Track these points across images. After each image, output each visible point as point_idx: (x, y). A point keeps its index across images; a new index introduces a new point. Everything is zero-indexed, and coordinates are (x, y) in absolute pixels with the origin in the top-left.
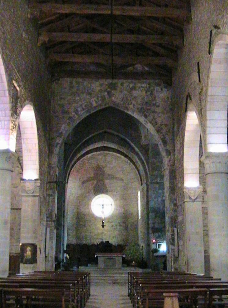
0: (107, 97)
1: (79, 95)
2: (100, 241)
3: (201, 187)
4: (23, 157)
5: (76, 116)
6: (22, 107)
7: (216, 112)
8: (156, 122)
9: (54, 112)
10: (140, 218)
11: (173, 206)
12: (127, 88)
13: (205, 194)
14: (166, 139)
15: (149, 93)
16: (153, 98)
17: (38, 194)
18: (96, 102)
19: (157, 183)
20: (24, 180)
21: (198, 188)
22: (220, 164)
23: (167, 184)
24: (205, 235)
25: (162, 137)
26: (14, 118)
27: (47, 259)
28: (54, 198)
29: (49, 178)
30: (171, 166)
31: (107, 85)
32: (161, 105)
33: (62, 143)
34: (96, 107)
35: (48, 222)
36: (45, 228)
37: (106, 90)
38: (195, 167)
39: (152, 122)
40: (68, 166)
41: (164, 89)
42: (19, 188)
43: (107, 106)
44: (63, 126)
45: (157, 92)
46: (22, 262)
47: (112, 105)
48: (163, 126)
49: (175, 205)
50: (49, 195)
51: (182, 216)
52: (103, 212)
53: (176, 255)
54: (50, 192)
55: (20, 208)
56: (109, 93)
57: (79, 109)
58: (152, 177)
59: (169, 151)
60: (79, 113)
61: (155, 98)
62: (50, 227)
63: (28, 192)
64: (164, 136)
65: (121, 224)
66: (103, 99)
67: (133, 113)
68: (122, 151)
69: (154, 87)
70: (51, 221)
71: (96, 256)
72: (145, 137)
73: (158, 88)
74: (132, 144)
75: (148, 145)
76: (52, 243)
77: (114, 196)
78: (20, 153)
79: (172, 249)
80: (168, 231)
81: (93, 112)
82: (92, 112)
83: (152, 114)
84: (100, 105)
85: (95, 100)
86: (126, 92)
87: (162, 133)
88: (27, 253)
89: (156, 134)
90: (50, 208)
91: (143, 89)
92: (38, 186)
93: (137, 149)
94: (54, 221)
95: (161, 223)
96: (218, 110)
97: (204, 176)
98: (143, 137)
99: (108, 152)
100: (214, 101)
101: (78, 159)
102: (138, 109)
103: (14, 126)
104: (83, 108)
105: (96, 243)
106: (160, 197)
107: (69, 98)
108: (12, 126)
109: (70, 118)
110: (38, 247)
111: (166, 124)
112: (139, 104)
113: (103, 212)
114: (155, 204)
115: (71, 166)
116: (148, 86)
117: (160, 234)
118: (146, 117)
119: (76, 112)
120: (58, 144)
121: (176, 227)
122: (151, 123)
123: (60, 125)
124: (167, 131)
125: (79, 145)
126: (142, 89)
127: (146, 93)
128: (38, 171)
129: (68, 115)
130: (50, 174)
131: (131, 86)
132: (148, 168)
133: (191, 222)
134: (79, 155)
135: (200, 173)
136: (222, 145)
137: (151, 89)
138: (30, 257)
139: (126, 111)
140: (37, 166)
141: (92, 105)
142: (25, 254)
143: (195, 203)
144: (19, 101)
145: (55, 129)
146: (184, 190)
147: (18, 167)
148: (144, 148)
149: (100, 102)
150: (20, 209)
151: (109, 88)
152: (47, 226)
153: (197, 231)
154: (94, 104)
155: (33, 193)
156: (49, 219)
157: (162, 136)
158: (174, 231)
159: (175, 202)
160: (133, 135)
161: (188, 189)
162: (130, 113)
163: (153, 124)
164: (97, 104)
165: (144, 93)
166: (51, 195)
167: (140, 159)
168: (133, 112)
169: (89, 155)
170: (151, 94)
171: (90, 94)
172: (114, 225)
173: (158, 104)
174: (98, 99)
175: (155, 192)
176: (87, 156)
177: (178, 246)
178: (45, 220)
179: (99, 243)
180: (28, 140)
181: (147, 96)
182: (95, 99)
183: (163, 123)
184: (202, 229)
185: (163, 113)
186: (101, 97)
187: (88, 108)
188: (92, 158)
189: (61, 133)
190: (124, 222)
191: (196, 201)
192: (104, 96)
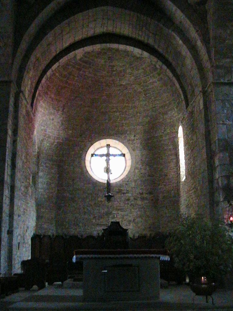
10: (183, 178)
52: (107, 170)
65: (145, 196)
68: (146, 41)
71: (74, 259)
77: (131, 142)
93: (179, 15)
105: (95, 234)
113: (107, 170)
132: (209, 52)
175: (228, 105)
179: (101, 234)
188: (86, 62)
190: (150, 193)
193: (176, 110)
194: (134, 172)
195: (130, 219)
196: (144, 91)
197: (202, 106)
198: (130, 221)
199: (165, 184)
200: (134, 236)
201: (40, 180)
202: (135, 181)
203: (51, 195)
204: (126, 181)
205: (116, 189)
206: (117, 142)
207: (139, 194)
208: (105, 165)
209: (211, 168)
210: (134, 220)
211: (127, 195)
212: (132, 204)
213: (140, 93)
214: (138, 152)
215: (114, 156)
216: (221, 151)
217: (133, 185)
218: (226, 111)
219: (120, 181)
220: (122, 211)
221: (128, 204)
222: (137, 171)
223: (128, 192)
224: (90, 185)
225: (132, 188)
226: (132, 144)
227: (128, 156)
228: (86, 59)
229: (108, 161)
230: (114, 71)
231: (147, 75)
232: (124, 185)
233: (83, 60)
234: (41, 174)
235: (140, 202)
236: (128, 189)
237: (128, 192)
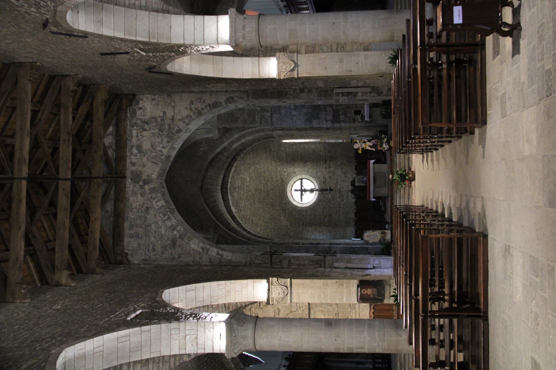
0: (152, 186)
1: (150, 225)
2: (350, 193)
3: (277, 54)
4: (237, 301)
5: (178, 229)
6: (165, 305)
7: (172, 30)
8: (187, 117)
9: (174, 259)
11: (304, 94)
12: (138, 157)
13: (288, 49)
14: (211, 103)
15: (146, 127)
16: (153, 120)
17: (289, 280)
18: (159, 200)
19: (271, 116)
20: (268, 299)
21: (278, 59)
22: (246, 26)
23: (274, 102)
24: (344, 49)
25: (208, 108)
26: (181, 316)
27: (376, 266)
28: (294, 257)
29: (267, 265)
30: (248, 96)
31: (134, 186)
32: (163, 110)
33: (216, 247)
34: (167, 202)
35: (326, 266)
36: (334, 270)
37: (142, 187)
38: (251, 64)
39: (187, 122)
40: (248, 239)
41: (141, 105)
42: (280, 307)
43: (164, 184)
44: (193, 246)
45: (144, 115)
46: (382, 300)
47: (164, 178)
48: (193, 107)
49: (302, 91)
50: (290, 263)
51: (317, 81)
53: (369, 90)
54: (285, 263)
55: (307, 304)
56: (146, 182)
57: (169, 224)
58: (263, 123)
59: (227, 98)
60: (174, 224)
61: (153, 118)
62: (333, 262)
63: (286, 293)
64: (206, 106)
65: (327, 166)
66: (153, 190)
67: (174, 148)
68: (228, 164)
69: (137, 119)
70: (325, 261)
72: (208, 132)
73: (139, 112)
74: (218, 150)
75: (219, 129)
76: (354, 259)
77: (289, 175)
78: (231, 307)
79: (362, 96)
80: (338, 101)
81: (172, 204)
82: (174, 207)
83: (176, 122)
84: (163, 194)
85: (156, 203)
86: (145, 159)
87: (203, 109)
88: (369, 293)
89: (205, 117)
90: (307, 262)
91: (141, 135)
92: (278, 280)
93: (225, 144)
94: (325, 257)
95: (326, 112)
96: (171, 27)
97: (262, 51)
98: (207, 136)
99: (229, 184)
100: (158, 32)
101: (239, 224)
102: (168, 142)
103: (194, 315)
104: (167, 219)
105: (354, 200)
106: (291, 112)
107: (152, 239)
108: (193, 319)
109: (181, 237)
110: (360, 278)
111: (190, 103)
112: (162, 140)
113: (312, 191)
115: (249, 235)
116: (135, 128)
117: (341, 113)
118: (179, 131)
119: (173, 228)
120: (218, 254)
121: (333, 90)
122: (188, 124)
123: (192, 252)
124: (199, 101)
125: (218, 223)
126: (140, 137)
127: (145, 130)
128: (255, 280)
129: (178, 240)
130: (260, 264)
131: (135, 151)
132: (251, 128)
133: (326, 68)
134: (234, 224)
135: (259, 57)
136: (219, 23)
137: (140, 124)
138: (375, 289)
139: (172, 159)
140: (250, 281)
141: (163, 206)
142: (372, 296)
143: (299, 63)
144: (157, 310)
145: (197, 258)
146: (282, 78)
147: (250, 309)
148: (224, 135)
149: (159, 195)
150: (309, 304)
151: (138, 183)
152: (333, 267)
153: (338, 61)
154: (162, 203)
155: (287, 287)
156: (322, 264)
157: (206, 108)
158: (338, 93)
159: (298, 91)
161: (279, 73)
162: (174, 153)
163: (190, 121)
164: (161, 198)
165: (145, 133)
166: (290, 261)
167: (239, 139)
168: (173, 148)
169: (234, 210)
170: (147, 123)
171: (148, 209)
172: (329, 175)
173: (162, 115)
174: (154, 199)
176: (234, 213)
177: (358, 87)
178: (323, 269)
179: (354, 196)
180: (212, 295)
181: (150, 129)
182: (154, 202)
183: (189, 107)
184: (336, 54)
185: (174, 107)
186: (151, 193)
187: (167, 212)
189: (203, 249)
191: (297, 61)
192: (150, 189)
194: (311, 173)
195: (343, 176)
196: (254, 165)
197: (281, 132)
198: (345, 176)
199: (319, 151)
201: (317, 237)
202: (317, 172)
203: (327, 230)
204: (317, 179)
205: (323, 185)
206: (289, 184)
208: (308, 193)
209: (319, 129)
210: (344, 173)
211: (326, 178)
212: (333, 175)
213: (255, 168)
214: (297, 170)
215: (302, 186)
216: (312, 124)
217: (319, 174)
218: (288, 120)
219: (317, 183)
221: (333, 177)
222: (310, 171)
223: (325, 177)
224: (320, 204)
225: (322, 174)
226: (291, 174)
227: (304, 176)
229: (305, 191)
230: (241, 186)
232: (320, 180)
234: (313, 237)
237: (325, 177)
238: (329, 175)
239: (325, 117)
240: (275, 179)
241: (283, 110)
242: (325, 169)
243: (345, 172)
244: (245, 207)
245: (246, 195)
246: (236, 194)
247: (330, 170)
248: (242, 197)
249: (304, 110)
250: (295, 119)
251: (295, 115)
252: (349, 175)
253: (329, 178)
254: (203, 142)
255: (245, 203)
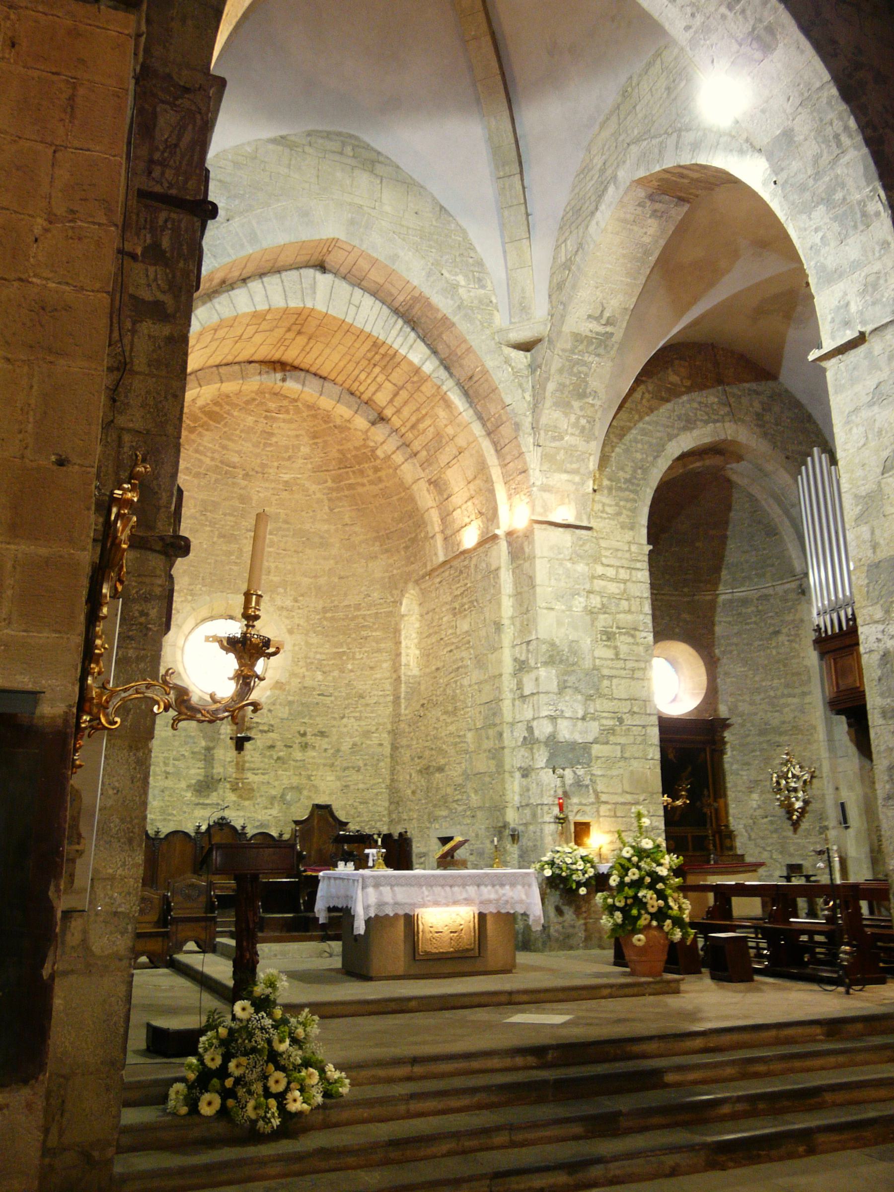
95: (583, 718)
105: (190, 829)
114: (560, 623)
117: (581, 772)
160: (461, 291)
179: (204, 828)
193: (403, 553)
195: (273, 792)
198: (274, 797)
199: (357, 714)
200: (281, 835)
207: (298, 736)
210: (283, 796)
211: (271, 735)
212: (279, 758)
220: (256, 774)
221: (271, 757)
226: (287, 618)
228: (217, 409)
230: (271, 445)
231: (346, 467)
233: (206, 409)
235: (300, 754)
236: (272, 722)
238: (279, 744)
239: (567, 715)
240: (273, 565)
241: (586, 569)
242: (299, 732)
243: (288, 797)
244: (197, 451)
245: (236, 459)
246: (250, 419)
247: (296, 746)
248: (231, 445)
249: (589, 641)
250: (559, 606)
251: (570, 609)
252: (274, 812)
253: (270, 743)
254: (482, 292)
255: (209, 454)
